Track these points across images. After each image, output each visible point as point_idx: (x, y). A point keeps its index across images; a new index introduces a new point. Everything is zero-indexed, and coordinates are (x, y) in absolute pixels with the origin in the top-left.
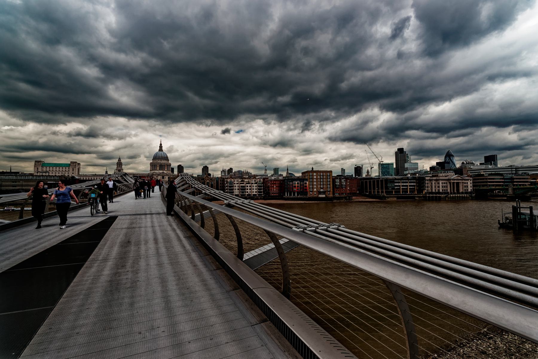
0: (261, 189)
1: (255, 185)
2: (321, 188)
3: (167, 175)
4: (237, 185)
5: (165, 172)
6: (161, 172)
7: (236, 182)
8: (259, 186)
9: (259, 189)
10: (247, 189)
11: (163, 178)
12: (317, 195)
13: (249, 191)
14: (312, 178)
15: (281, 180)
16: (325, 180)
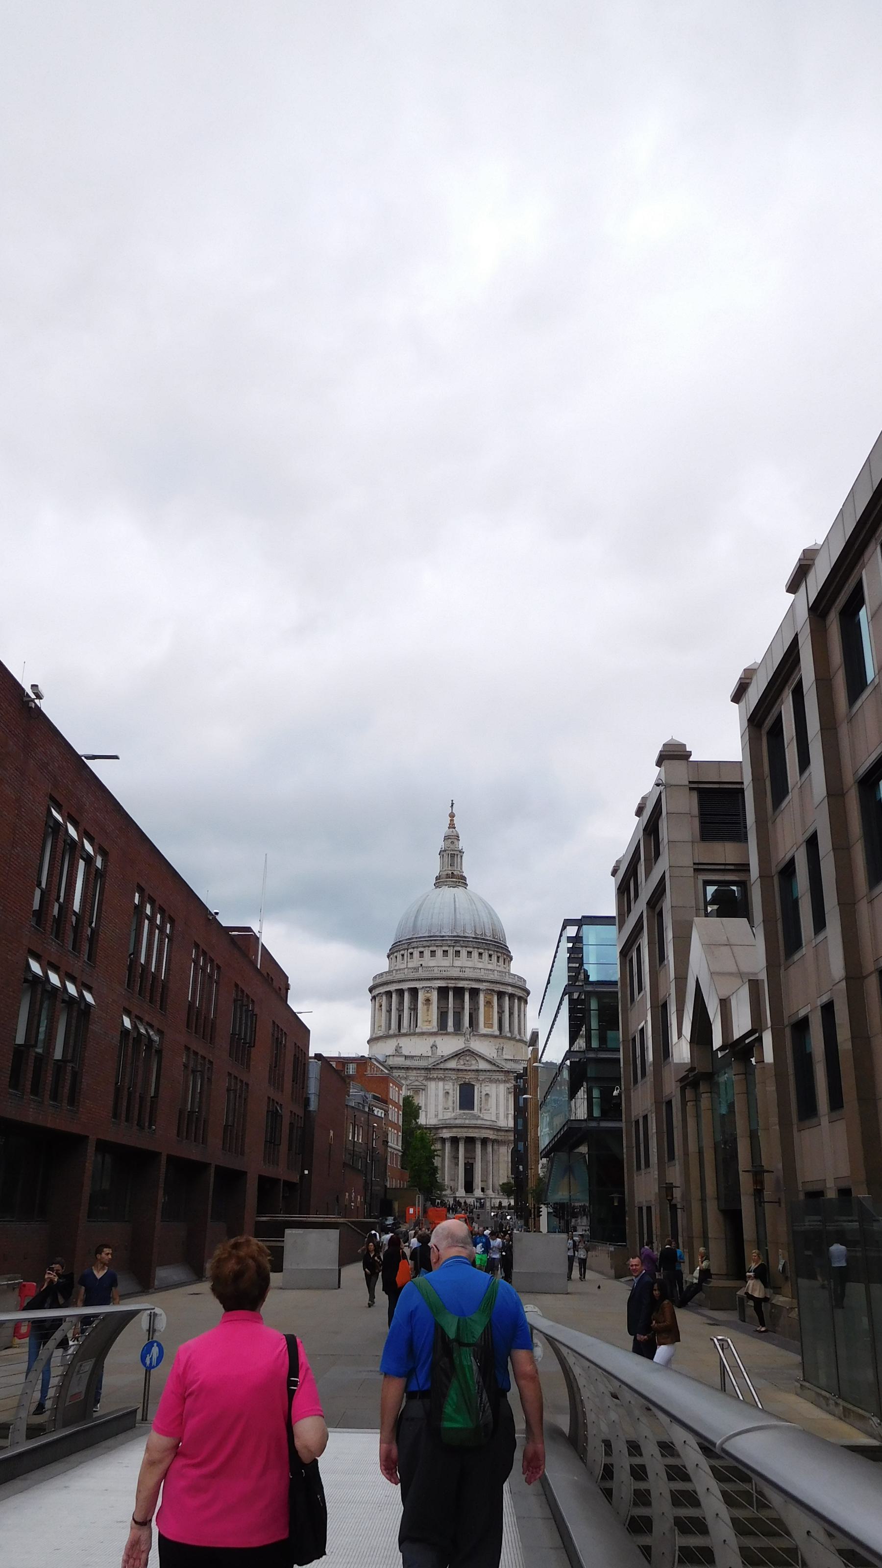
3: (498, 1071)
11: (467, 1099)
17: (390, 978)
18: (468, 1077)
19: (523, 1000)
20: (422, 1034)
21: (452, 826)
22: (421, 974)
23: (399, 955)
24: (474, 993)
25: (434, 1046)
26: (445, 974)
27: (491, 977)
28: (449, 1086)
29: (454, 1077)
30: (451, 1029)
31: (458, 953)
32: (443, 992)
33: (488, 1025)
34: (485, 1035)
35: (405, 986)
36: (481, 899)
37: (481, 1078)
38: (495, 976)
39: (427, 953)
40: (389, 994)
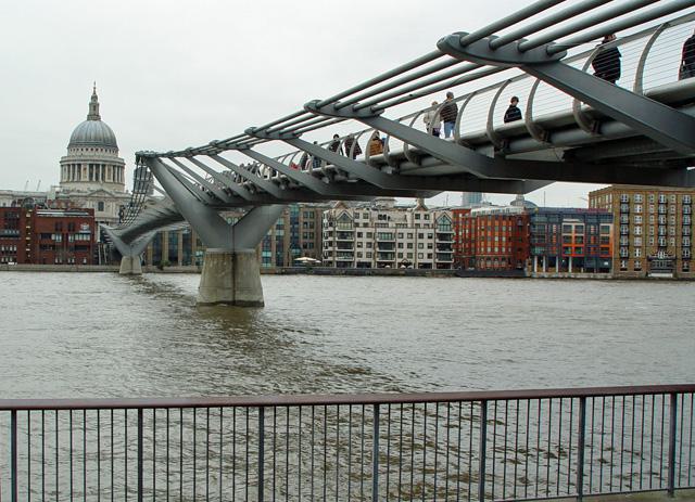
0: (448, 246)
1: (426, 232)
2: (659, 247)
4: (365, 231)
5: (107, 190)
6: (95, 187)
7: (361, 221)
8: (441, 237)
9: (441, 247)
10: (401, 245)
11: (101, 208)
12: (642, 273)
13: (405, 251)
14: (628, 213)
15: (520, 217)
16: (673, 220)
18: (102, 200)
19: (123, 168)
20: (84, 182)
32: (91, 166)
33: (109, 178)
36: (109, 129)
40: (69, 165)
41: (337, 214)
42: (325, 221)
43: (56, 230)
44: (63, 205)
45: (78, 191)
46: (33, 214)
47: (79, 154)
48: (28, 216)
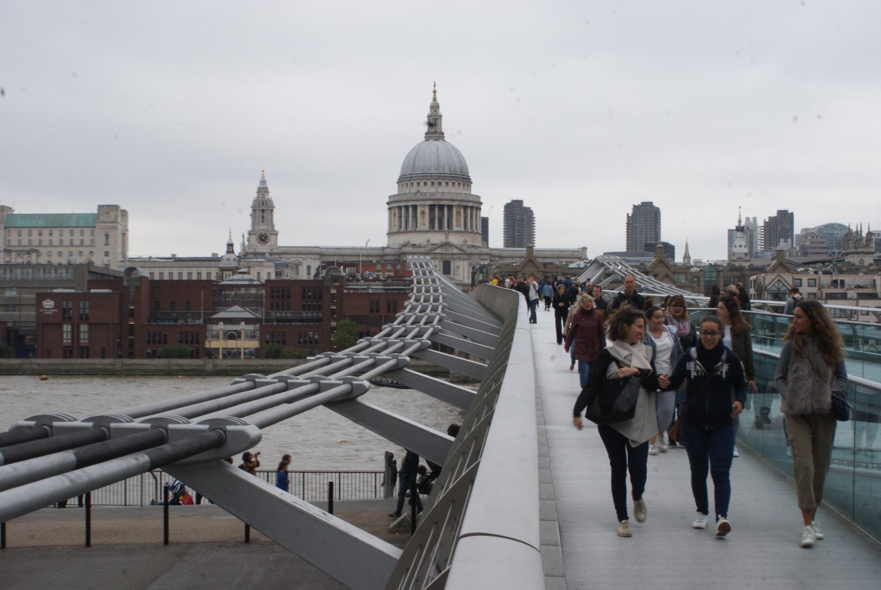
5: (454, 239)
6: (437, 238)
11: (447, 270)
17: (400, 198)
18: (447, 257)
20: (420, 232)
21: (435, 99)
22: (419, 196)
23: (405, 184)
24: (450, 207)
25: (428, 241)
26: (433, 197)
27: (460, 198)
28: (437, 262)
29: (439, 257)
30: (437, 228)
31: (440, 184)
32: (432, 208)
33: (458, 225)
34: (457, 232)
35: (410, 204)
37: (455, 257)
38: (462, 197)
39: (422, 183)
40: (400, 208)
41: (768, 280)
42: (752, 291)
43: (372, 311)
44: (389, 267)
45: (414, 245)
46: (340, 289)
47: (413, 190)
48: (333, 291)
